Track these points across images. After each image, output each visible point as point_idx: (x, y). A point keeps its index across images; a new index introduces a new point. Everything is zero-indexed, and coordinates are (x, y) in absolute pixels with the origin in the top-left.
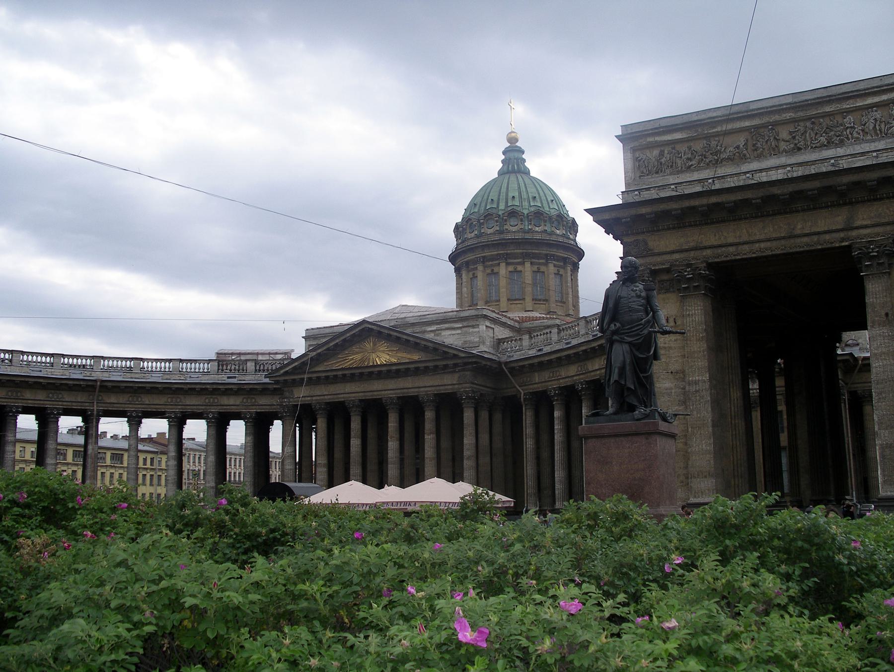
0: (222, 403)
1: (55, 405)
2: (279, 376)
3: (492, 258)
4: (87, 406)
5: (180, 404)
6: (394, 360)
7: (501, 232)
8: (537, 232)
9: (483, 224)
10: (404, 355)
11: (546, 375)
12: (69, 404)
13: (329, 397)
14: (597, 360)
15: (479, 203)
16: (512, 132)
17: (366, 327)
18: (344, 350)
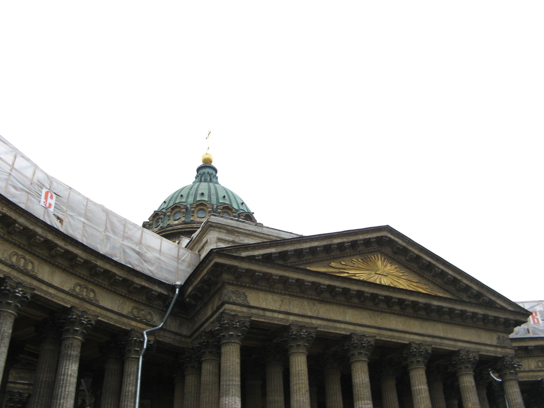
0: (40, 276)
2: (242, 259)
13: (320, 322)
17: (386, 237)
18: (340, 257)
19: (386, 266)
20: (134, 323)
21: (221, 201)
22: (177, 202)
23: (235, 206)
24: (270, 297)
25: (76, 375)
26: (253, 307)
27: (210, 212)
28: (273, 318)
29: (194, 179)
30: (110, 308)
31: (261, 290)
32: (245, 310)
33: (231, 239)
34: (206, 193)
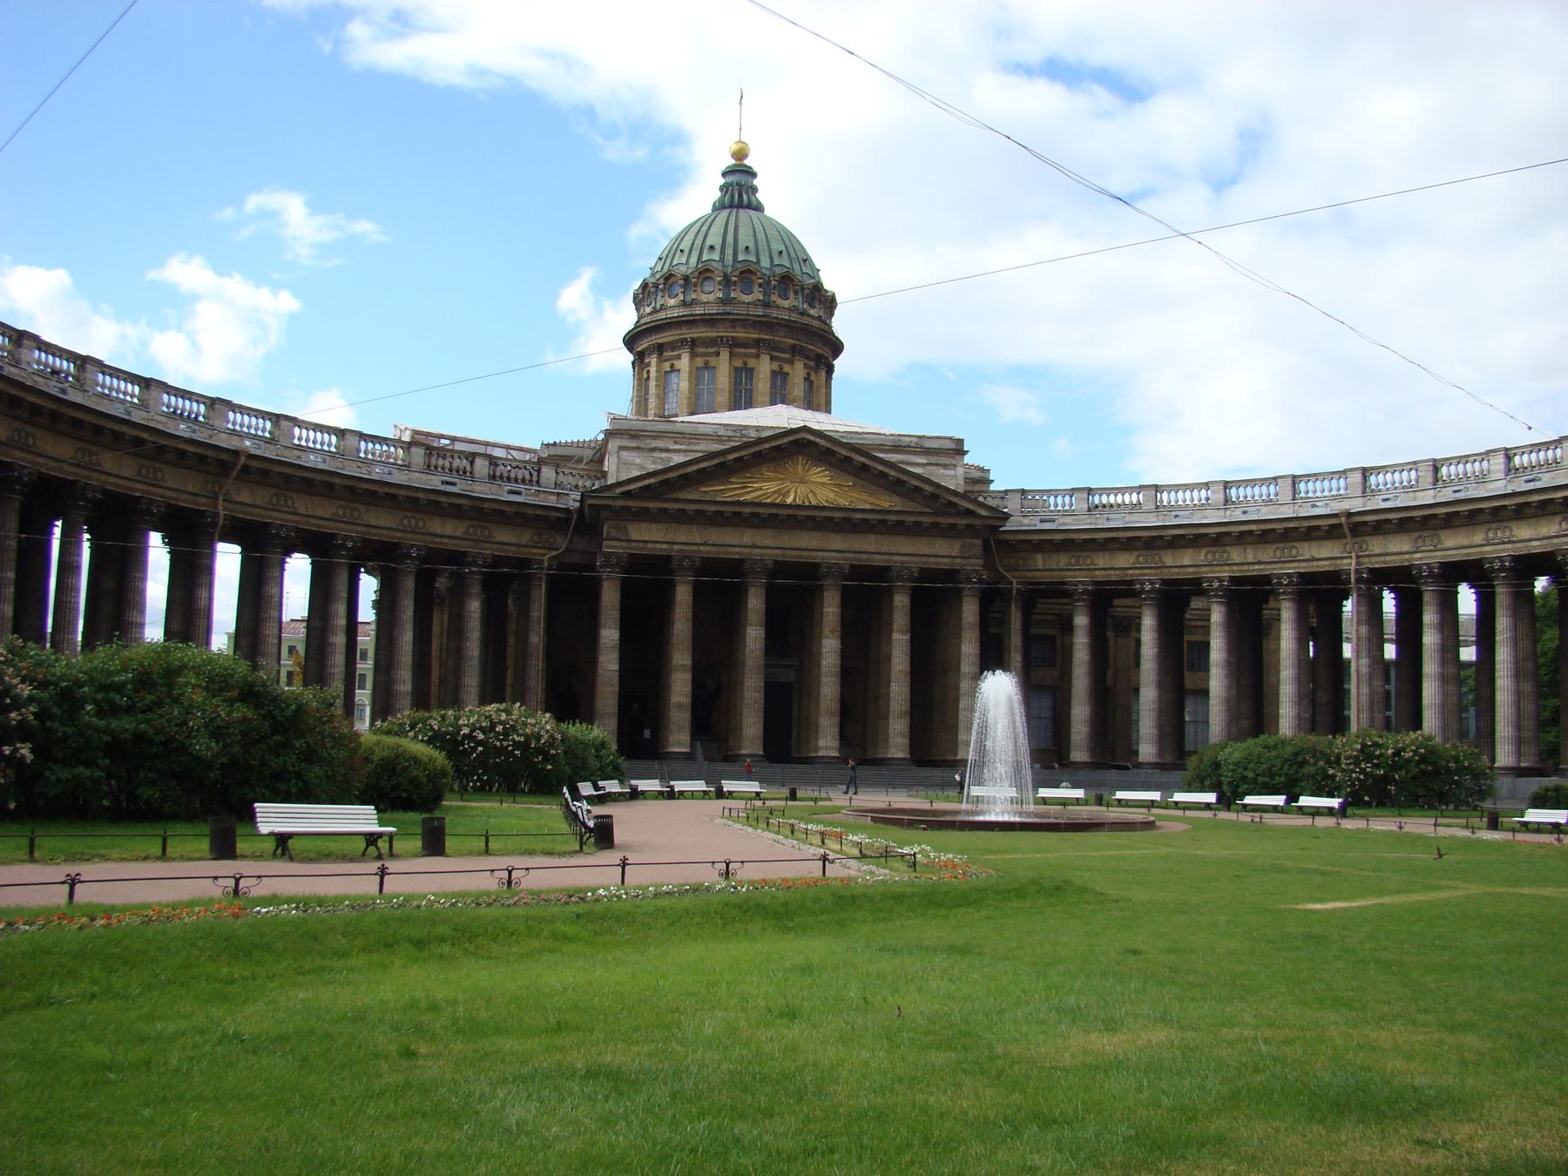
0: (432, 530)
1: (154, 494)
3: (744, 344)
4: (202, 504)
5: (359, 522)
6: (844, 502)
7: (766, 304)
8: (813, 317)
9: (735, 283)
10: (864, 496)
11: (1062, 560)
12: (174, 494)
13: (708, 548)
14: (1190, 552)
15: (718, 247)
16: (740, 142)
17: (803, 439)
19: (808, 470)
20: (535, 551)
21: (741, 257)
22: (675, 263)
23: (765, 262)
24: (654, 526)
25: (479, 611)
26: (634, 541)
27: (719, 283)
28: (655, 549)
29: (718, 194)
30: (507, 541)
31: (643, 521)
32: (624, 544)
33: (635, 445)
34: (718, 244)
